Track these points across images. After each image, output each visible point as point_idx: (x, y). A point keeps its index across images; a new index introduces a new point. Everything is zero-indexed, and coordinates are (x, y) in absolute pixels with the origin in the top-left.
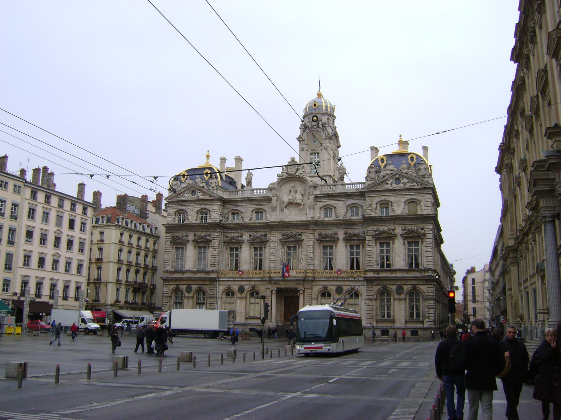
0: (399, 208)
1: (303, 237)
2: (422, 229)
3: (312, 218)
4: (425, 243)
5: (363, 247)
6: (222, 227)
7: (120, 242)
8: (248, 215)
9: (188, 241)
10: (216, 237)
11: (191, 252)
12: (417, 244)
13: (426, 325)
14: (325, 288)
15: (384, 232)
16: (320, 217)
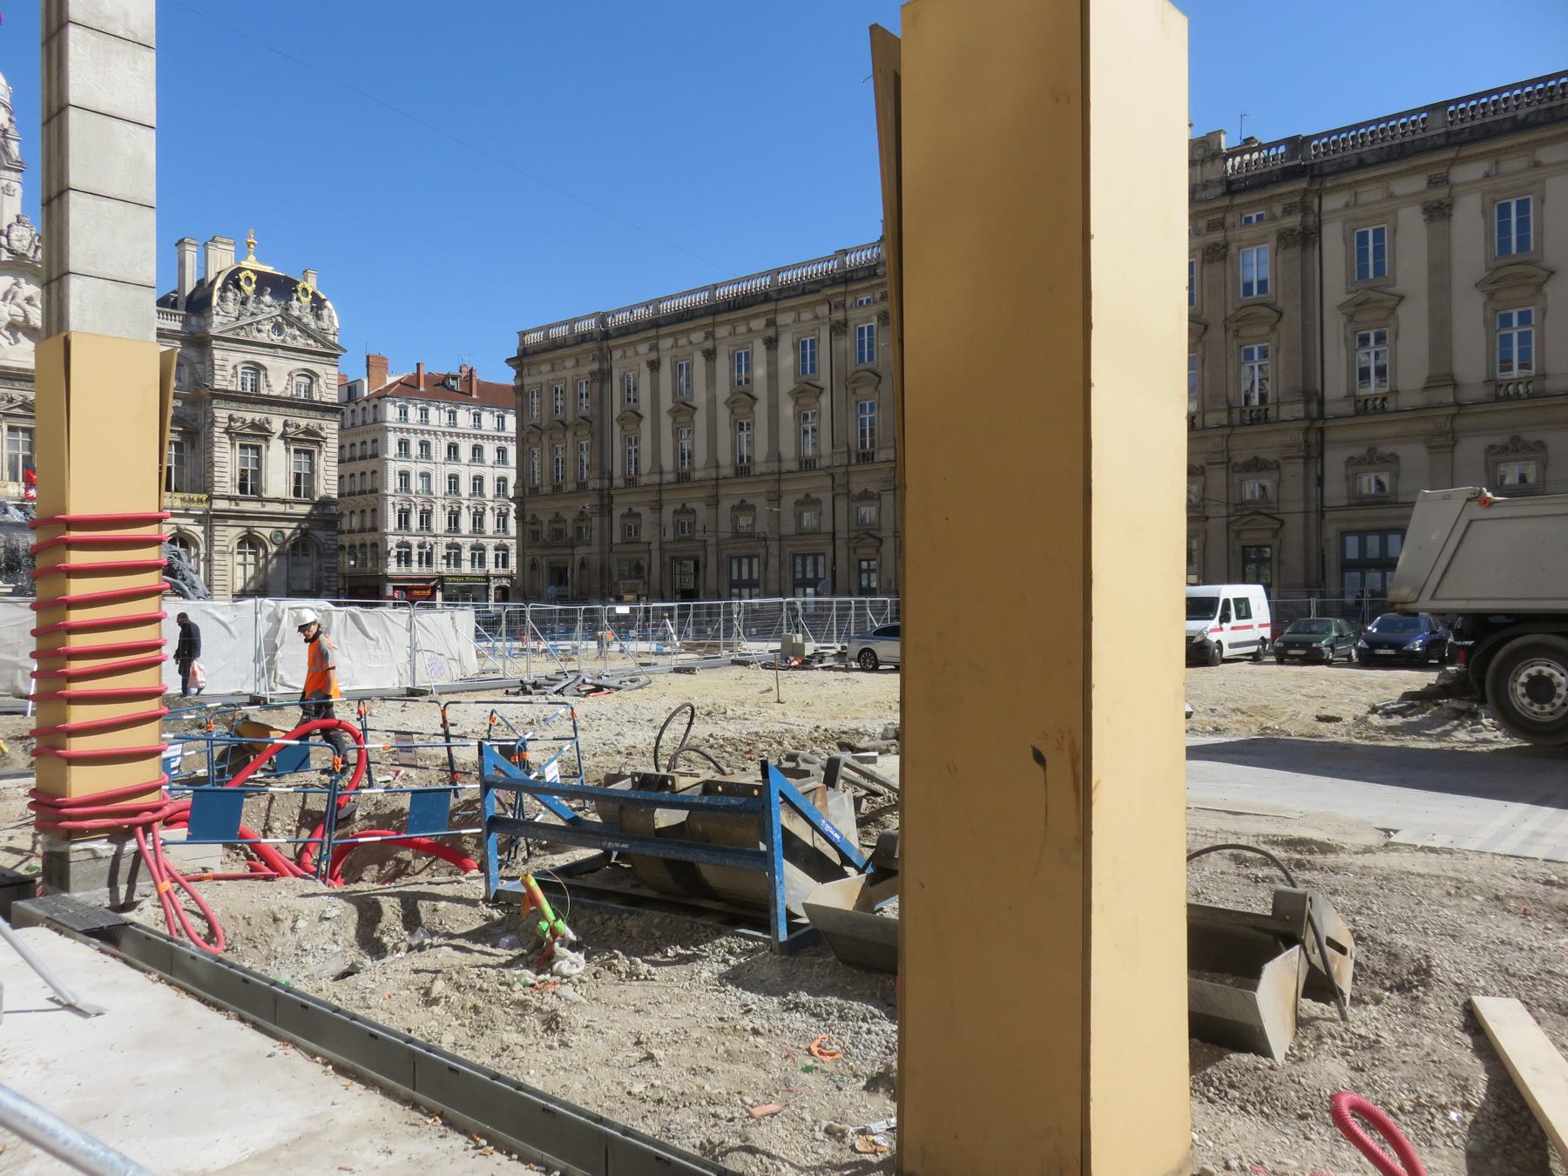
5: (193, 446)
15: (253, 425)
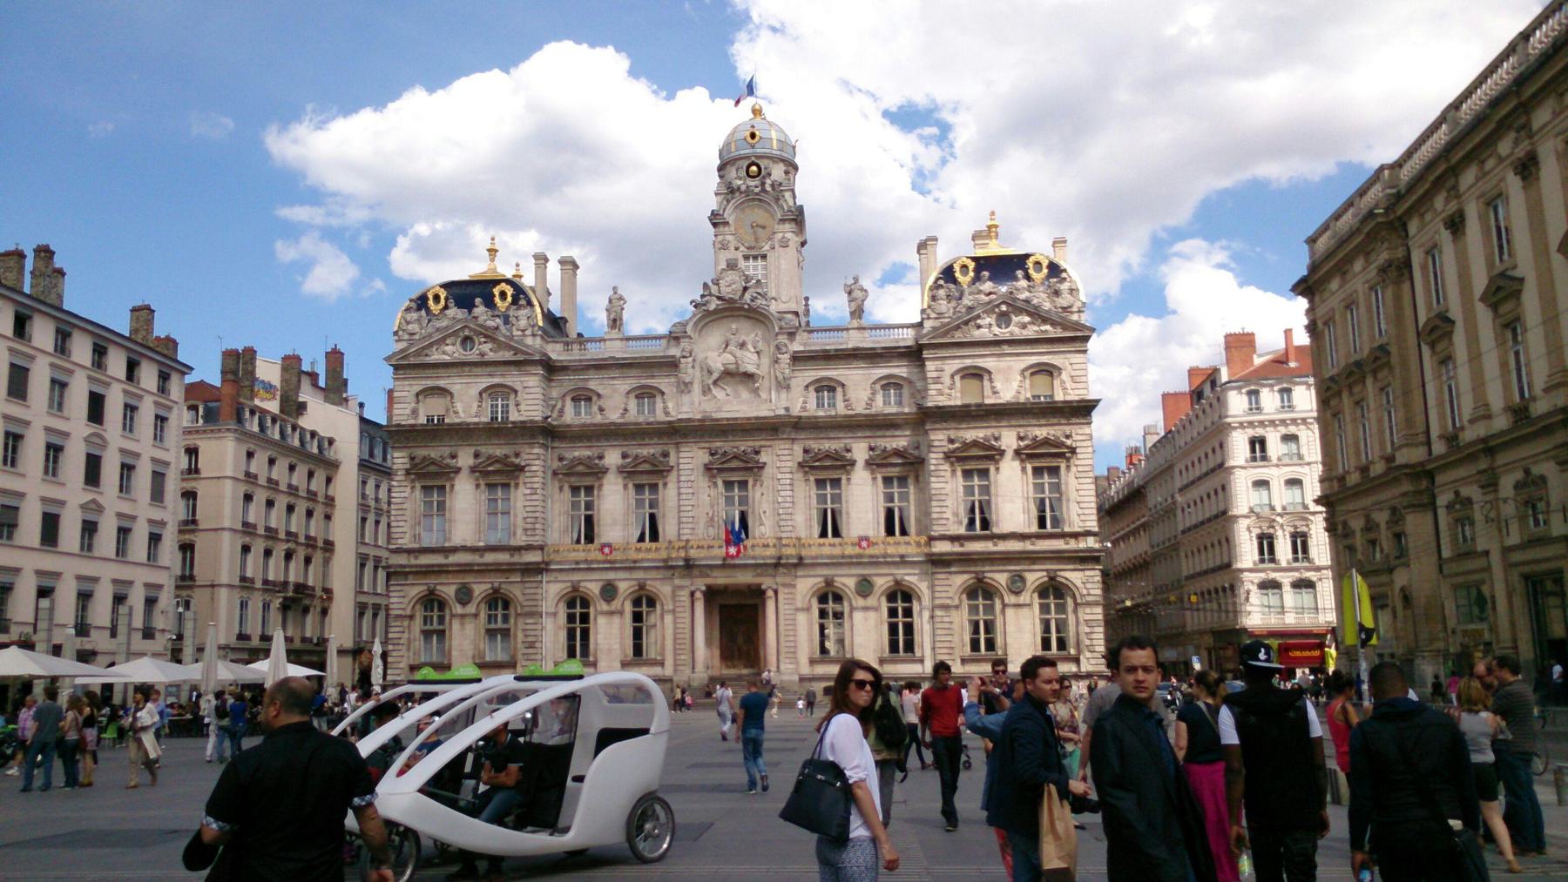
0: (1009, 382)
1: (763, 458)
2: (1068, 437)
3: (787, 409)
4: (1073, 469)
5: (917, 479)
6: (548, 433)
7: (248, 474)
8: (616, 401)
9: (458, 470)
10: (536, 459)
11: (465, 497)
12: (1054, 471)
13: (1086, 667)
14: (829, 582)
15: (975, 444)
16: (804, 409)
